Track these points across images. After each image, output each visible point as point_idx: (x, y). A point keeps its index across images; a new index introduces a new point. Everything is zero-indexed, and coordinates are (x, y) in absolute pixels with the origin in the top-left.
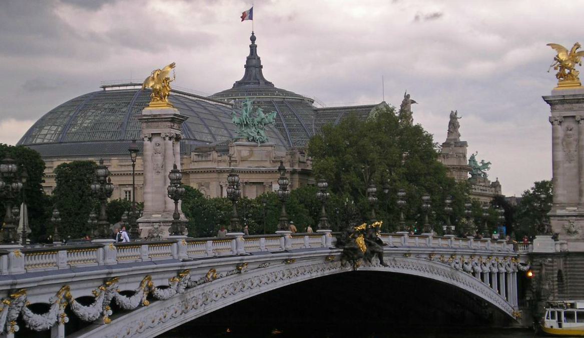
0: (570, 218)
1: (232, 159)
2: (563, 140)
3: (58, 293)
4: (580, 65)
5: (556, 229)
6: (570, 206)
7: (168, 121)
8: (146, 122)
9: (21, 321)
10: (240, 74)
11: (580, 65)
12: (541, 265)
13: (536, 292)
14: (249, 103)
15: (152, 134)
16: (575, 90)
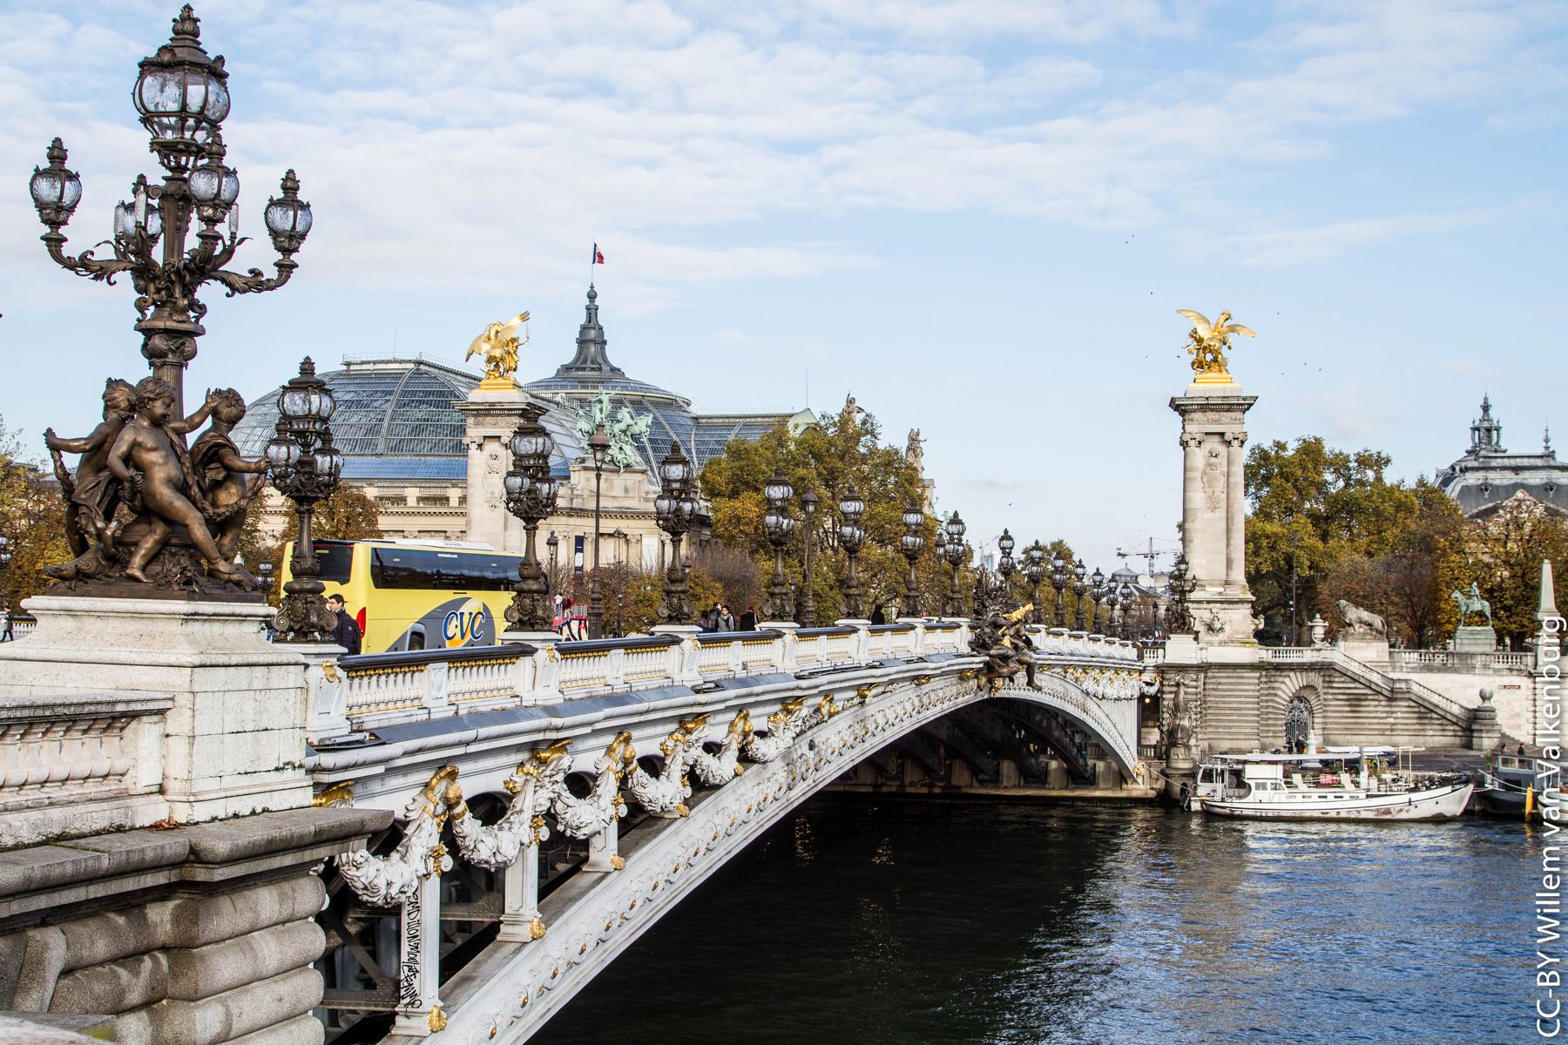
0: (1211, 605)
1: (575, 492)
2: (1204, 473)
3: (610, 750)
4: (1230, 348)
5: (1198, 626)
6: (1213, 585)
7: (514, 415)
8: (474, 415)
9: (551, 817)
10: (569, 354)
11: (1230, 348)
12: (1178, 685)
13: (1168, 731)
14: (605, 398)
15: (485, 437)
16: (1224, 390)
